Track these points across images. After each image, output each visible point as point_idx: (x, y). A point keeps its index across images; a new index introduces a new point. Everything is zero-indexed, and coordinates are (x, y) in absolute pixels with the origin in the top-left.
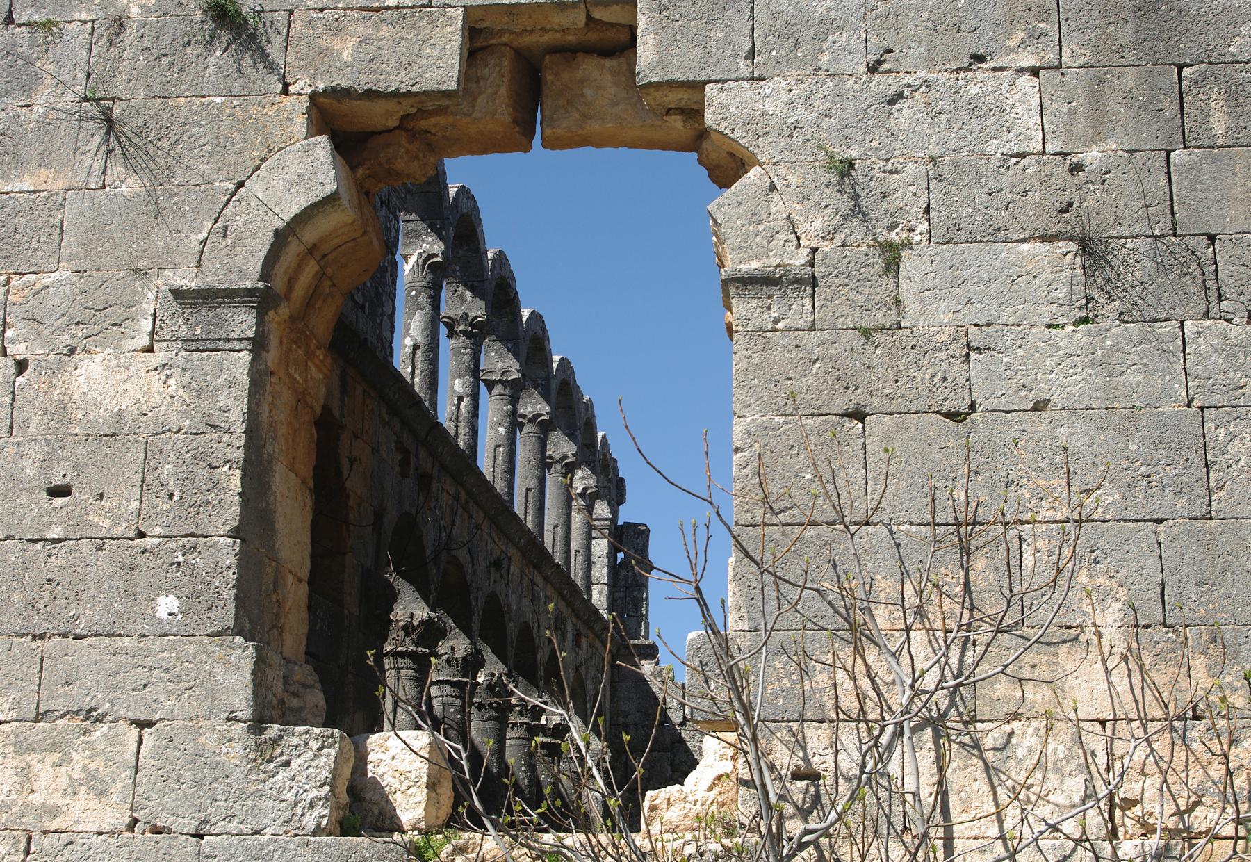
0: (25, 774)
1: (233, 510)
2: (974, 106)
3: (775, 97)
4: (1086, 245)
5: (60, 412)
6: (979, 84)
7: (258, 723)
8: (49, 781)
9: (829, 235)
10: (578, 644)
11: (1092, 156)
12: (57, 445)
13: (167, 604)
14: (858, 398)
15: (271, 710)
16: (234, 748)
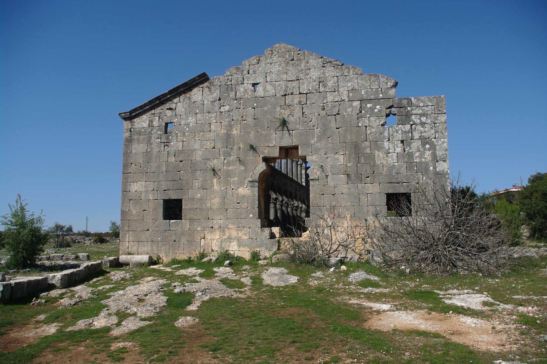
0: (238, 233)
1: (257, 205)
2: (336, 159)
3: (314, 158)
4: (348, 175)
5: (238, 194)
6: (337, 156)
7: (261, 227)
8: (240, 234)
9: (320, 174)
10: (300, 191)
11: (349, 165)
12: (237, 198)
13: (251, 215)
14: (323, 193)
15: (263, 226)
16: (259, 230)
